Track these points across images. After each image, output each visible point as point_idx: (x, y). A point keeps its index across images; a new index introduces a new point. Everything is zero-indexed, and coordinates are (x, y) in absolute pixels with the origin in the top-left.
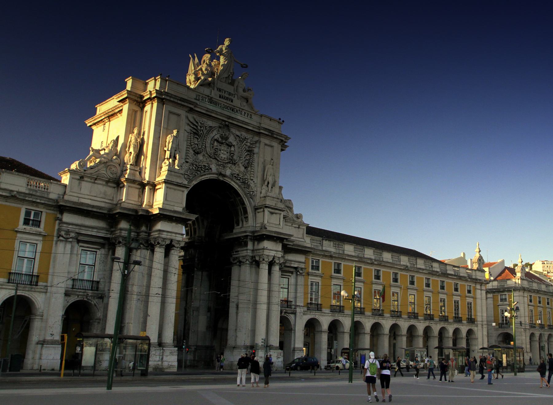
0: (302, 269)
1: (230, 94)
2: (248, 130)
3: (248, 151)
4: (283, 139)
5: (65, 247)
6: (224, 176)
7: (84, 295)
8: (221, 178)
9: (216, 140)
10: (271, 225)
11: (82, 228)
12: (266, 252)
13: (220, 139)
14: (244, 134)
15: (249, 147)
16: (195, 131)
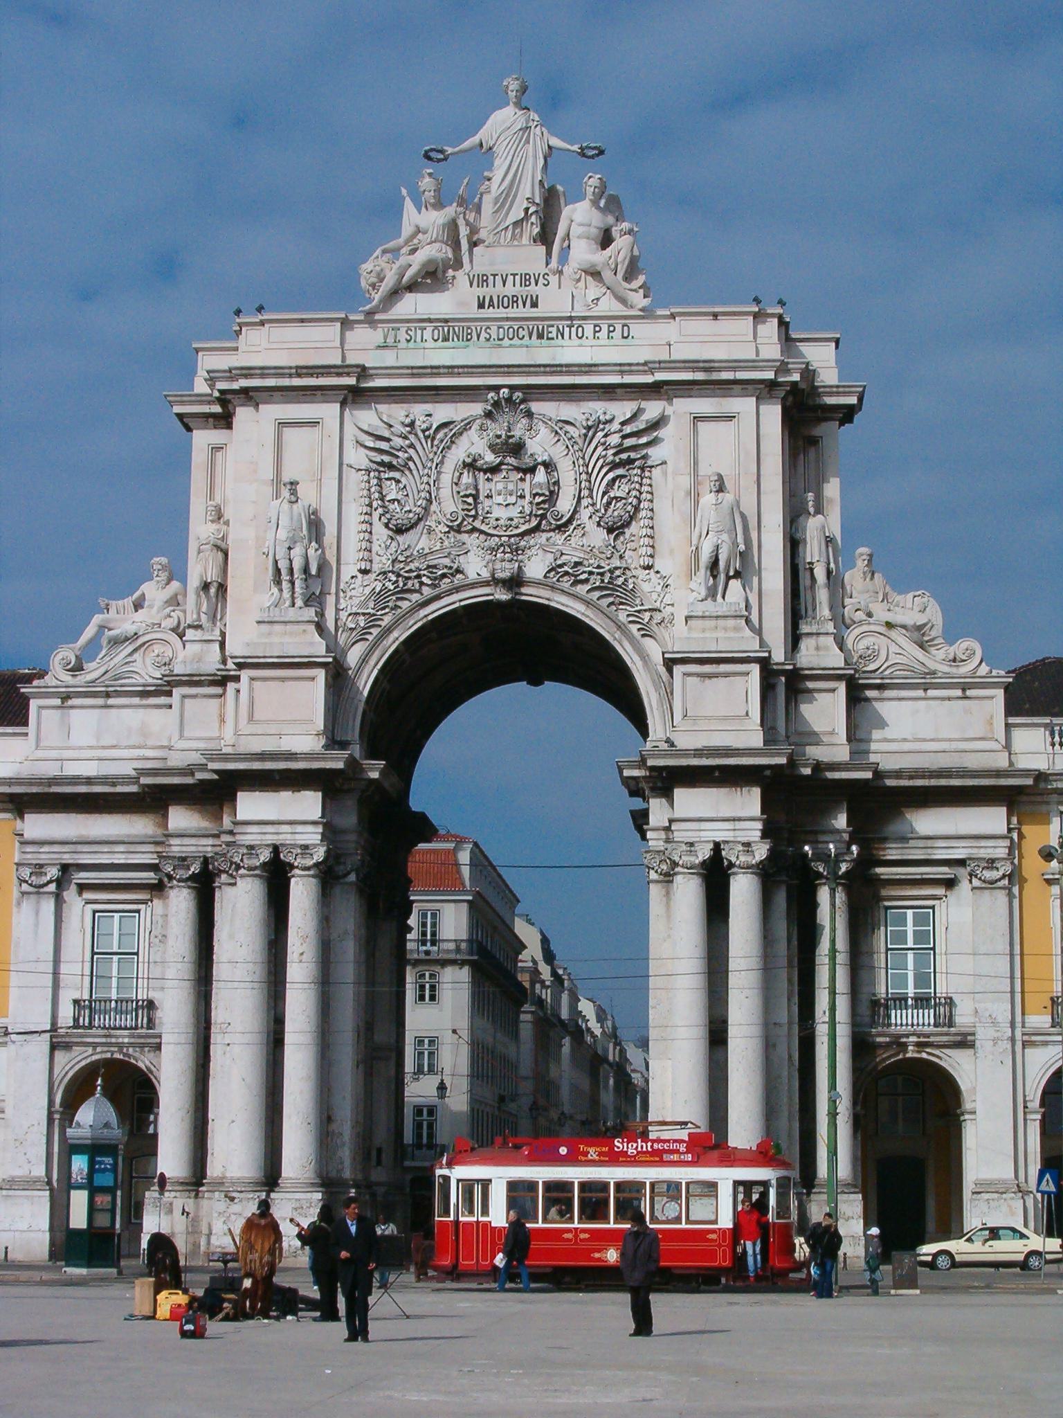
0: (991, 863)
1: (526, 280)
2: (608, 392)
3: (622, 464)
4: (770, 375)
5: (37, 913)
6: (515, 582)
7: (111, 1044)
8: (502, 596)
9: (465, 465)
10: (703, 725)
11: (80, 848)
12: (682, 833)
13: (490, 458)
14: (598, 408)
15: (621, 450)
16: (378, 458)
